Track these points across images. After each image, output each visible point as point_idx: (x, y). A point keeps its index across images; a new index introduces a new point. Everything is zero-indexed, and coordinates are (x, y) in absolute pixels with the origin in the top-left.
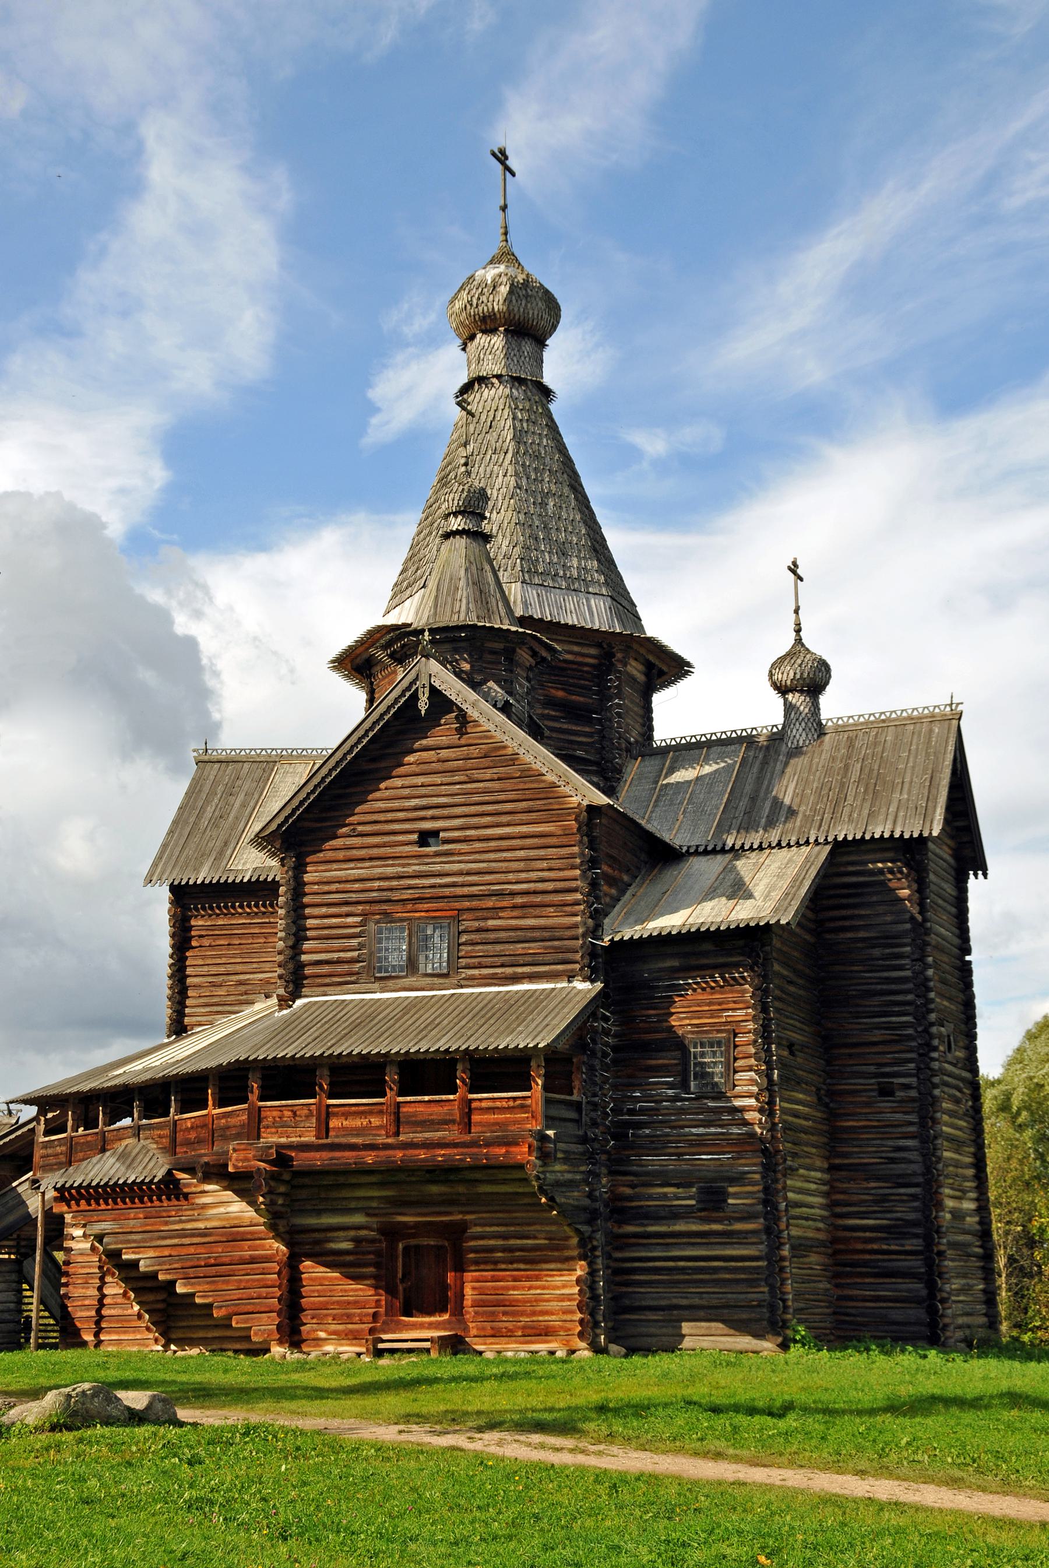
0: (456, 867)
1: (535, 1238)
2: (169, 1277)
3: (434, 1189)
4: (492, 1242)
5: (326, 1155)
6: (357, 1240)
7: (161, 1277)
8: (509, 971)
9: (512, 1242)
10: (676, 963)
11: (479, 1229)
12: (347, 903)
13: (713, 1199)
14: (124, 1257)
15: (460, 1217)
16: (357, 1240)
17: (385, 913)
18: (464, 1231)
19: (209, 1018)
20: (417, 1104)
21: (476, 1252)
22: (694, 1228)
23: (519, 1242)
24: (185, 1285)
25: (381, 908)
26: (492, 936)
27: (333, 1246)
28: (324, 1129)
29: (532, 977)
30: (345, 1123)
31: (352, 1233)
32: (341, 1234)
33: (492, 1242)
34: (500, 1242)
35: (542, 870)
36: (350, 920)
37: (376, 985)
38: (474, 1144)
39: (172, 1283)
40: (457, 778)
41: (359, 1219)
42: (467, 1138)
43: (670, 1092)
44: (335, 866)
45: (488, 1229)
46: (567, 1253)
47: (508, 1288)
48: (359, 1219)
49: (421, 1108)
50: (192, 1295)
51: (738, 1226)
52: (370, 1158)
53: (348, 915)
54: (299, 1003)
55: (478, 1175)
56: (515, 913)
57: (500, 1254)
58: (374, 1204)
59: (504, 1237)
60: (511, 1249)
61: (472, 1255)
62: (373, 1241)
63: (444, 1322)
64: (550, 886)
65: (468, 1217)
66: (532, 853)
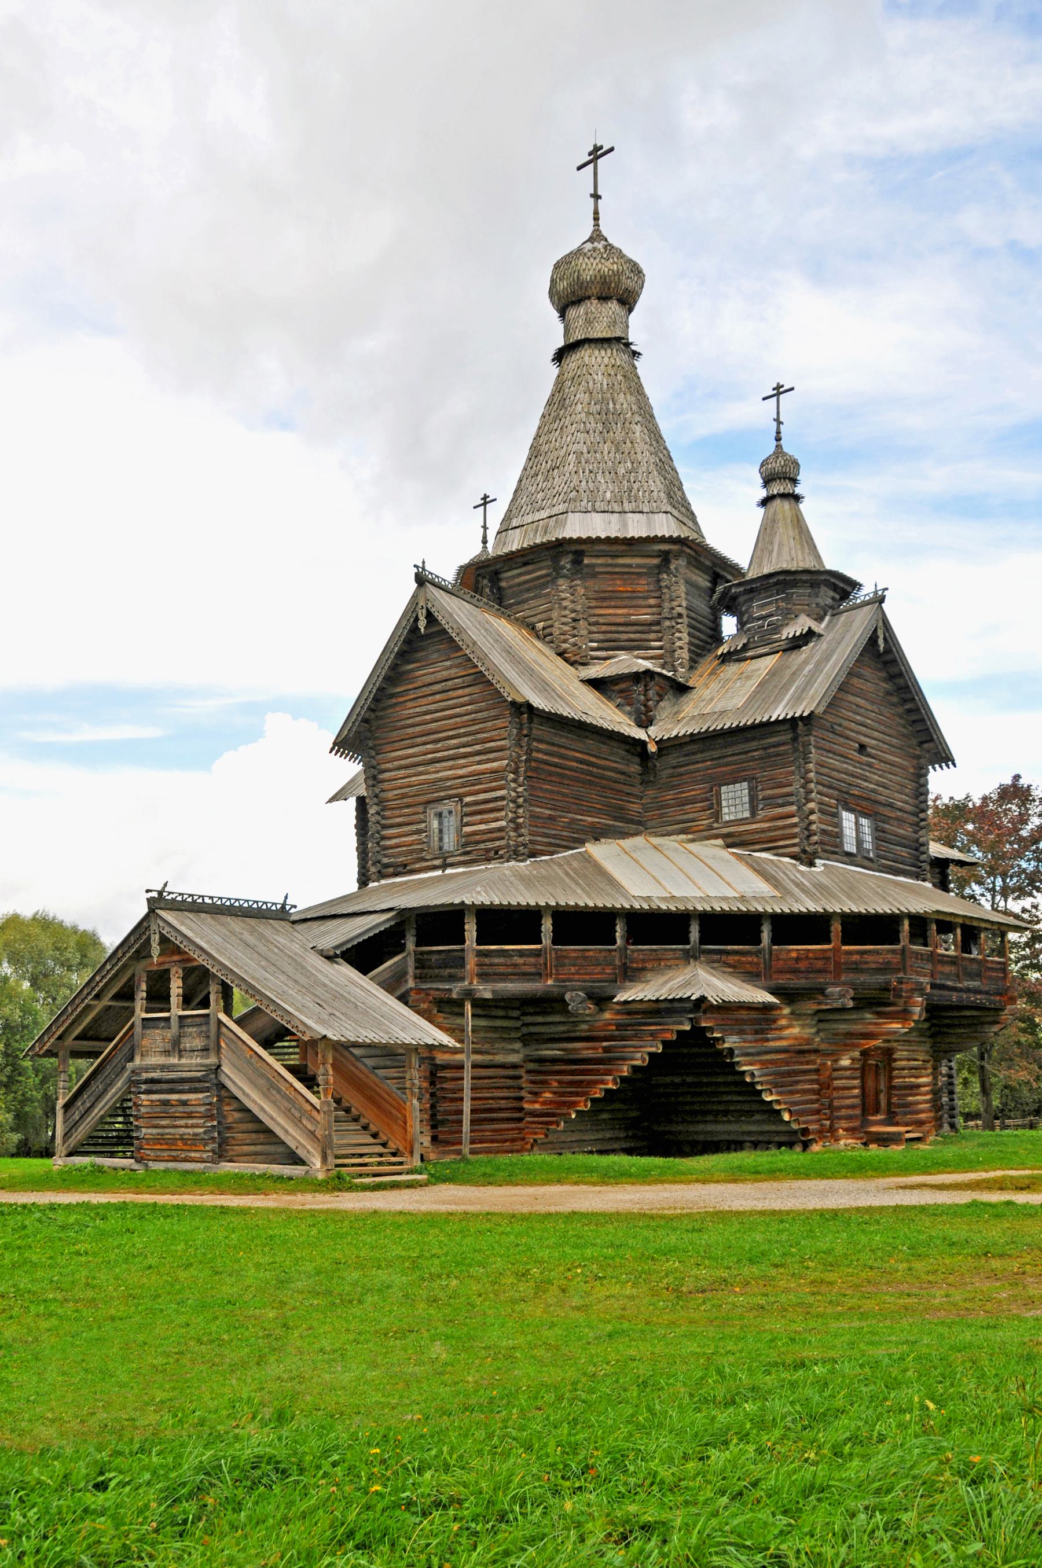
12: (830, 787)
16: (853, 1059)
19: (552, 849)
59: (909, 1060)
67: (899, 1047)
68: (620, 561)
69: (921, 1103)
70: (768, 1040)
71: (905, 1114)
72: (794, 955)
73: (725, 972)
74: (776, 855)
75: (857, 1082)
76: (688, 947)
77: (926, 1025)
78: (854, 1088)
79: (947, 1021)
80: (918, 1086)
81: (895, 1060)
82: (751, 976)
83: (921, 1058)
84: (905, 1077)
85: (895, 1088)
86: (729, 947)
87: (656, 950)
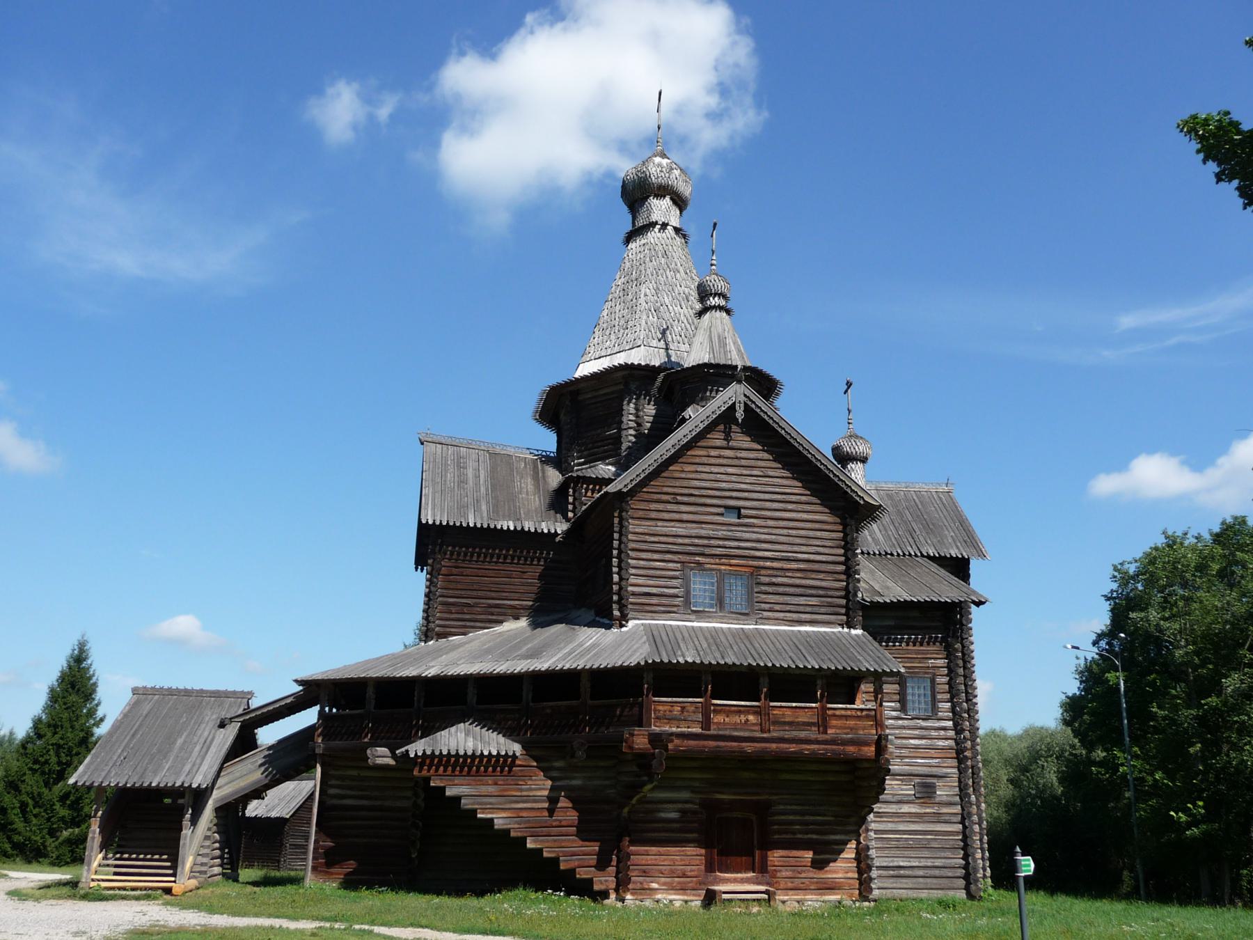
0: (754, 536)
1: (825, 815)
2: (519, 834)
3: (746, 775)
4: (791, 817)
5: (712, 743)
7: (513, 834)
8: (795, 616)
9: (807, 818)
10: (891, 623)
13: (926, 791)
16: (683, 812)
17: (698, 563)
20: (783, 709)
22: (913, 810)
24: (535, 842)
25: (693, 557)
26: (781, 589)
27: (663, 815)
28: (706, 723)
29: (812, 623)
31: (680, 806)
32: (671, 806)
33: (791, 817)
36: (671, 565)
37: (693, 617)
38: (833, 742)
39: (524, 840)
40: (755, 473)
41: (685, 795)
42: (821, 737)
43: (894, 714)
44: (660, 523)
48: (685, 795)
49: (788, 712)
50: (541, 850)
51: (945, 810)
52: (749, 747)
54: (631, 623)
56: (798, 575)
58: (697, 784)
59: (803, 814)
62: (694, 813)
65: (775, 798)
66: (811, 533)
68: (601, 392)
82: (509, 733)
84: (794, 833)
86: (495, 706)
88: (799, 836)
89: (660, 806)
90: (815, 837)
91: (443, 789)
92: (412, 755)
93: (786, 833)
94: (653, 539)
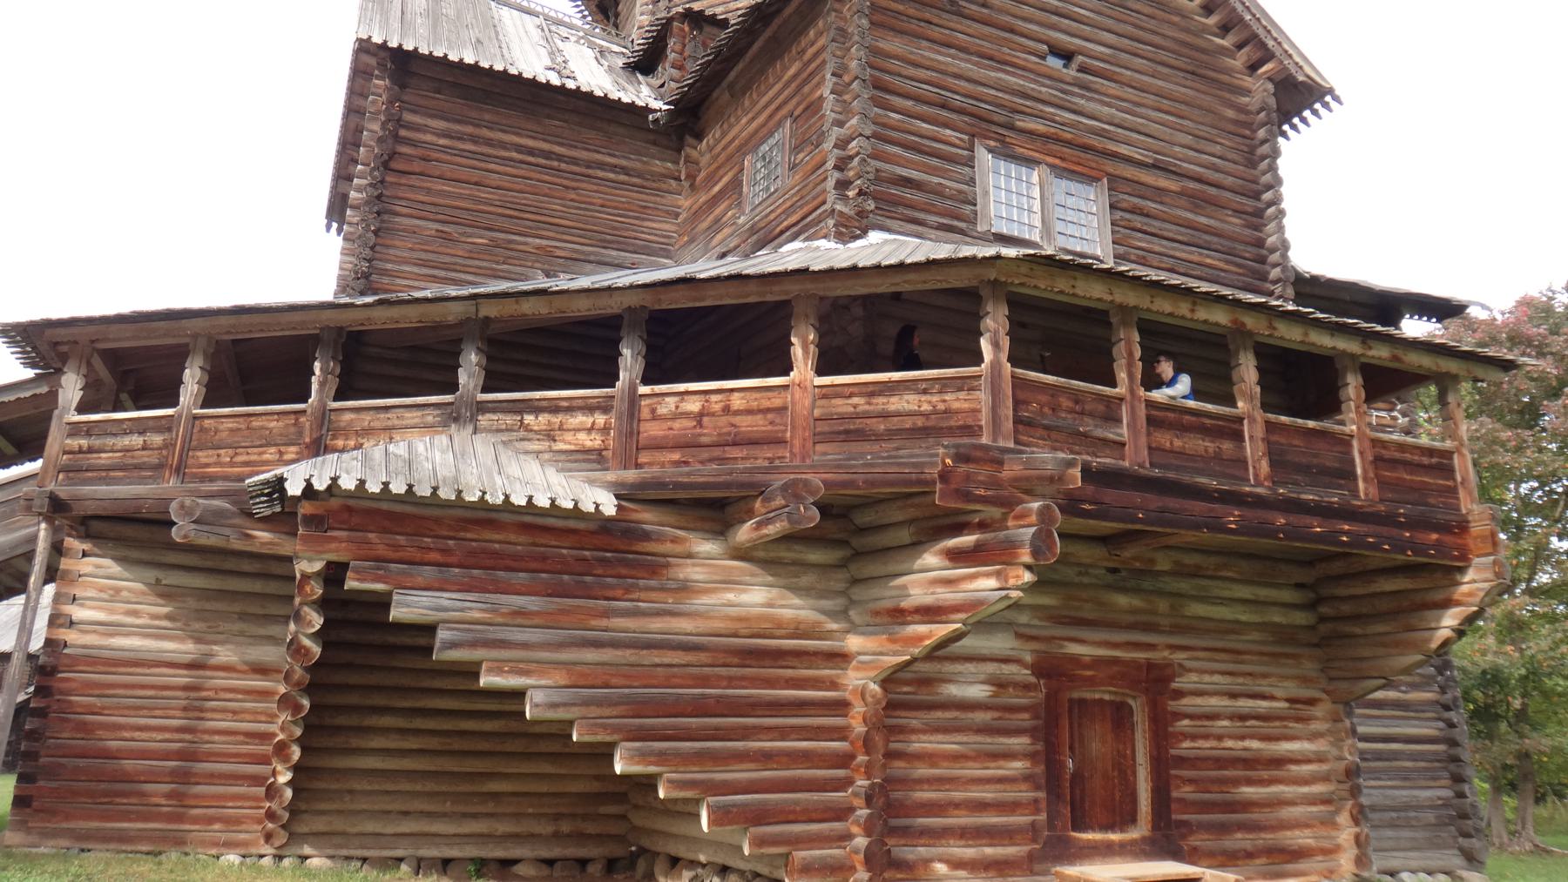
1: (1272, 698)
3: (1122, 600)
6: (1000, 684)
11: (1194, 677)
14: (485, 680)
15: (1166, 653)
16: (1000, 684)
18: (1171, 678)
21: (1191, 717)
23: (1250, 703)
24: (643, 756)
27: (954, 691)
30: (1178, 443)
31: (991, 668)
32: (970, 667)
34: (1226, 702)
35: (1214, 155)
39: (604, 754)
45: (1207, 678)
46: (1316, 726)
47: (1237, 782)
53: (946, 126)
55: (1184, 585)
57: (1225, 723)
59: (1233, 696)
60: (1243, 718)
61: (1186, 722)
62: (1027, 687)
63: (1133, 842)
64: (1229, 181)
65: (1179, 656)
67: (1188, 664)
69: (1292, 803)
70: (606, 614)
71: (1223, 829)
72: (693, 406)
73: (527, 452)
74: (806, 240)
75: (1020, 742)
76: (448, 398)
77: (1301, 618)
78: (1009, 755)
79: (1346, 608)
80: (1279, 762)
81: (1180, 694)
83: (1278, 693)
84: (1220, 738)
85: (1182, 761)
87: (387, 408)
88: (1229, 743)
89: (959, 667)
90: (1255, 744)
91: (383, 602)
92: (294, 488)
93: (1206, 737)
94: (912, 71)
